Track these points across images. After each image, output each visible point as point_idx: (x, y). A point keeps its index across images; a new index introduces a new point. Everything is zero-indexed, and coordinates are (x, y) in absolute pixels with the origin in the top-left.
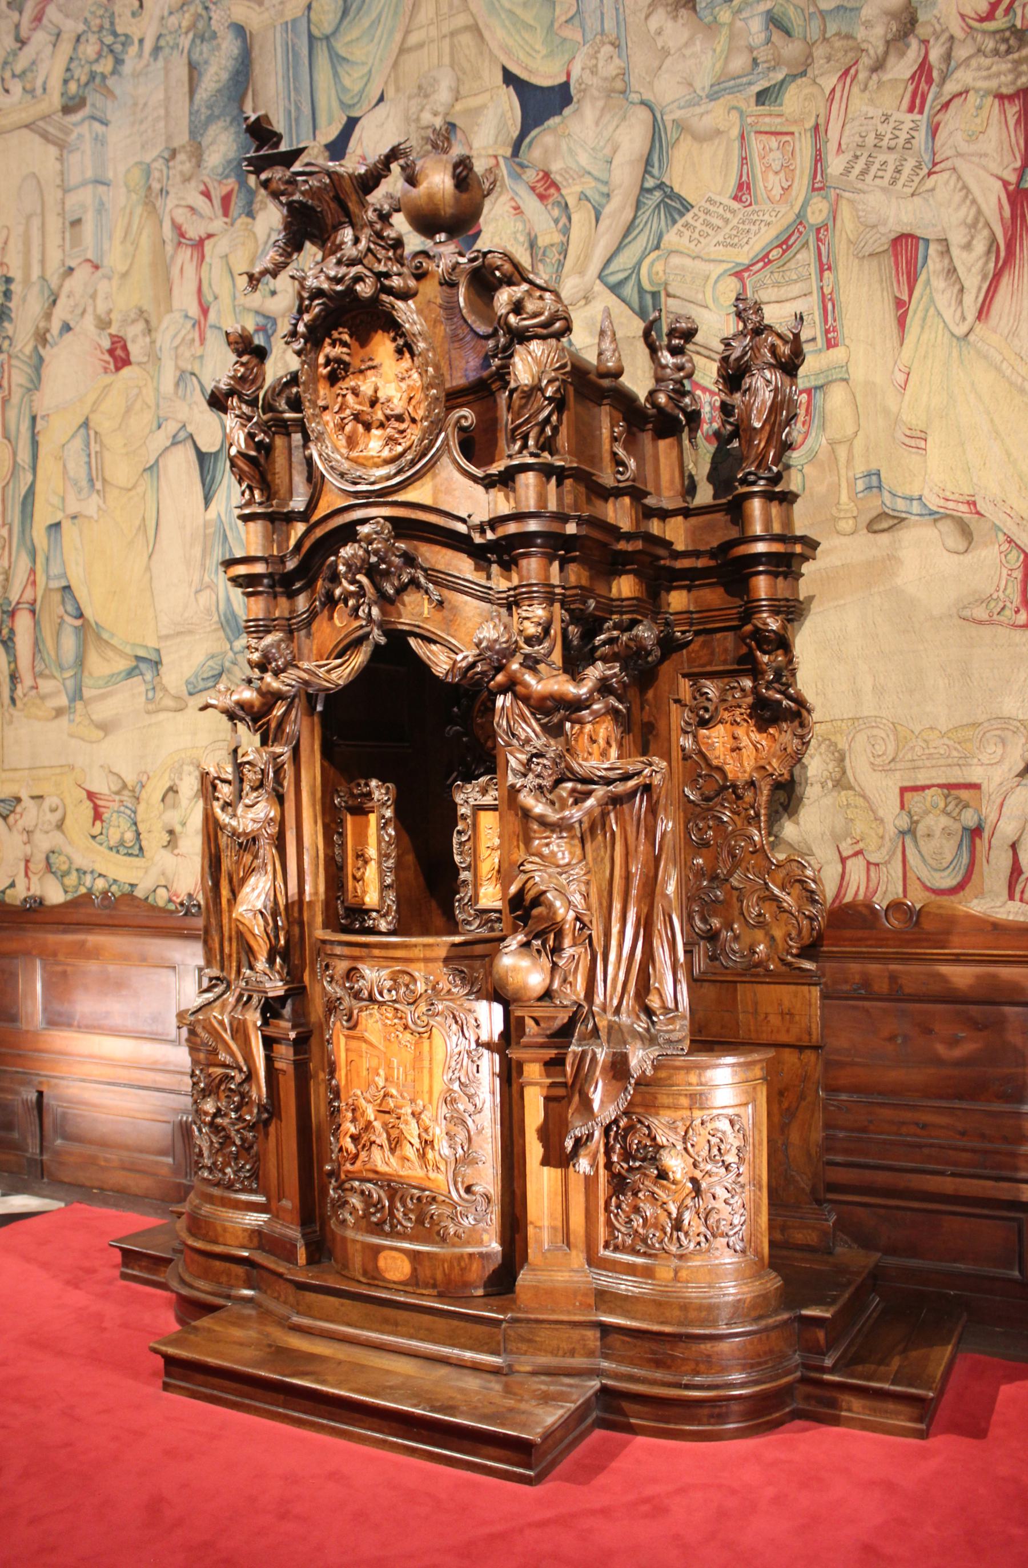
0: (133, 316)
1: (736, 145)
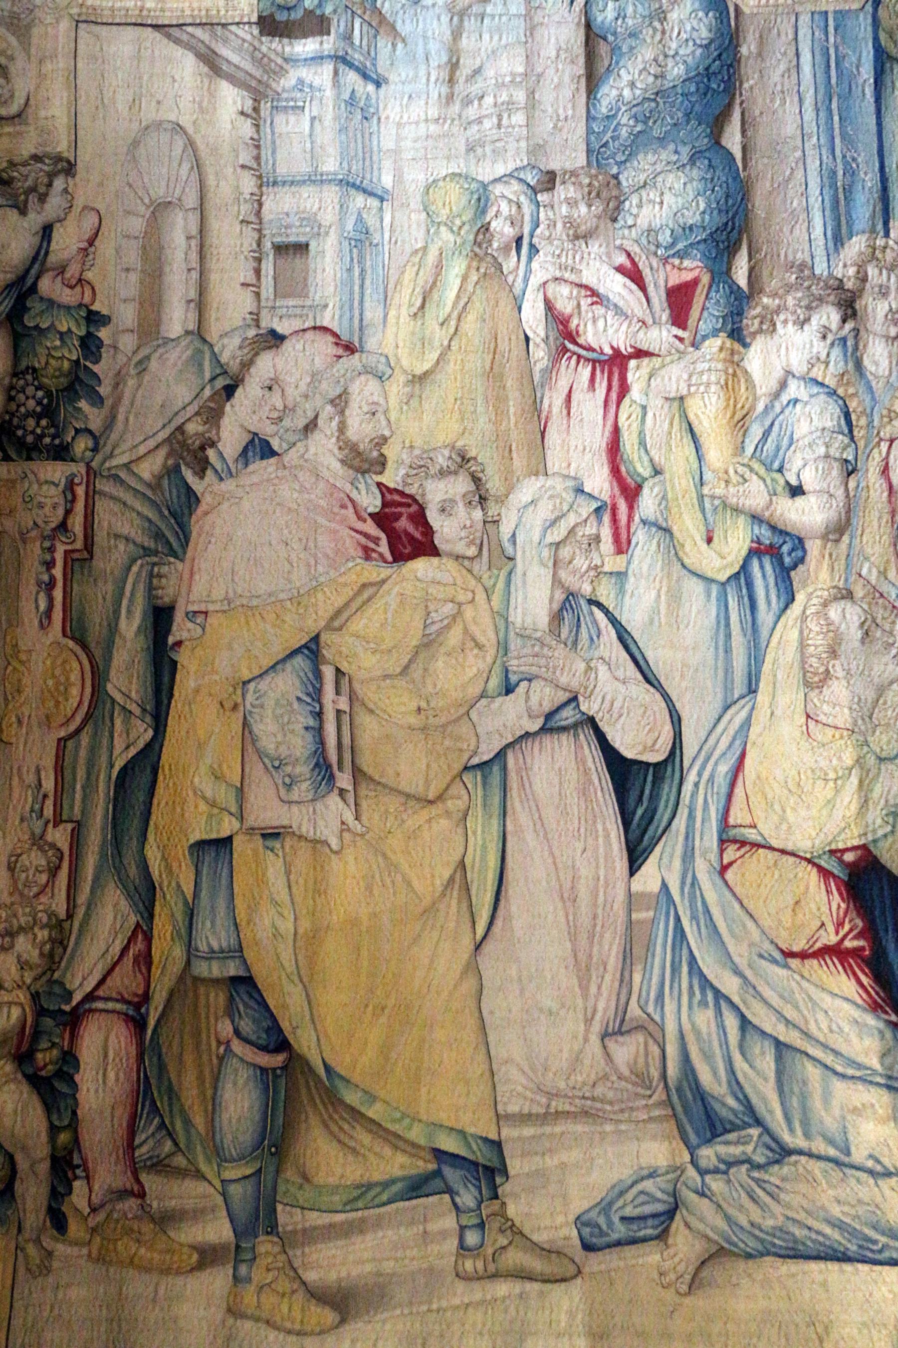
0: (441, 461)
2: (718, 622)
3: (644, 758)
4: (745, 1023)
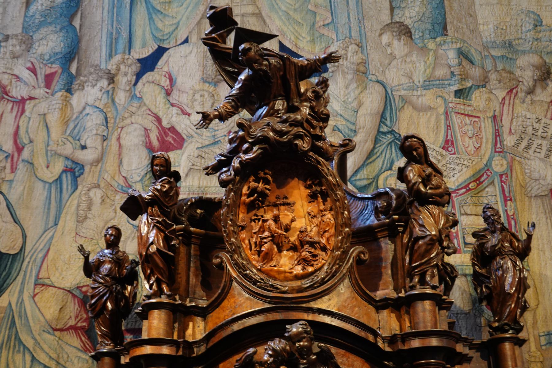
1: (443, 117)
2: (47, 198)
3: (9, 252)
4: (33, 359)
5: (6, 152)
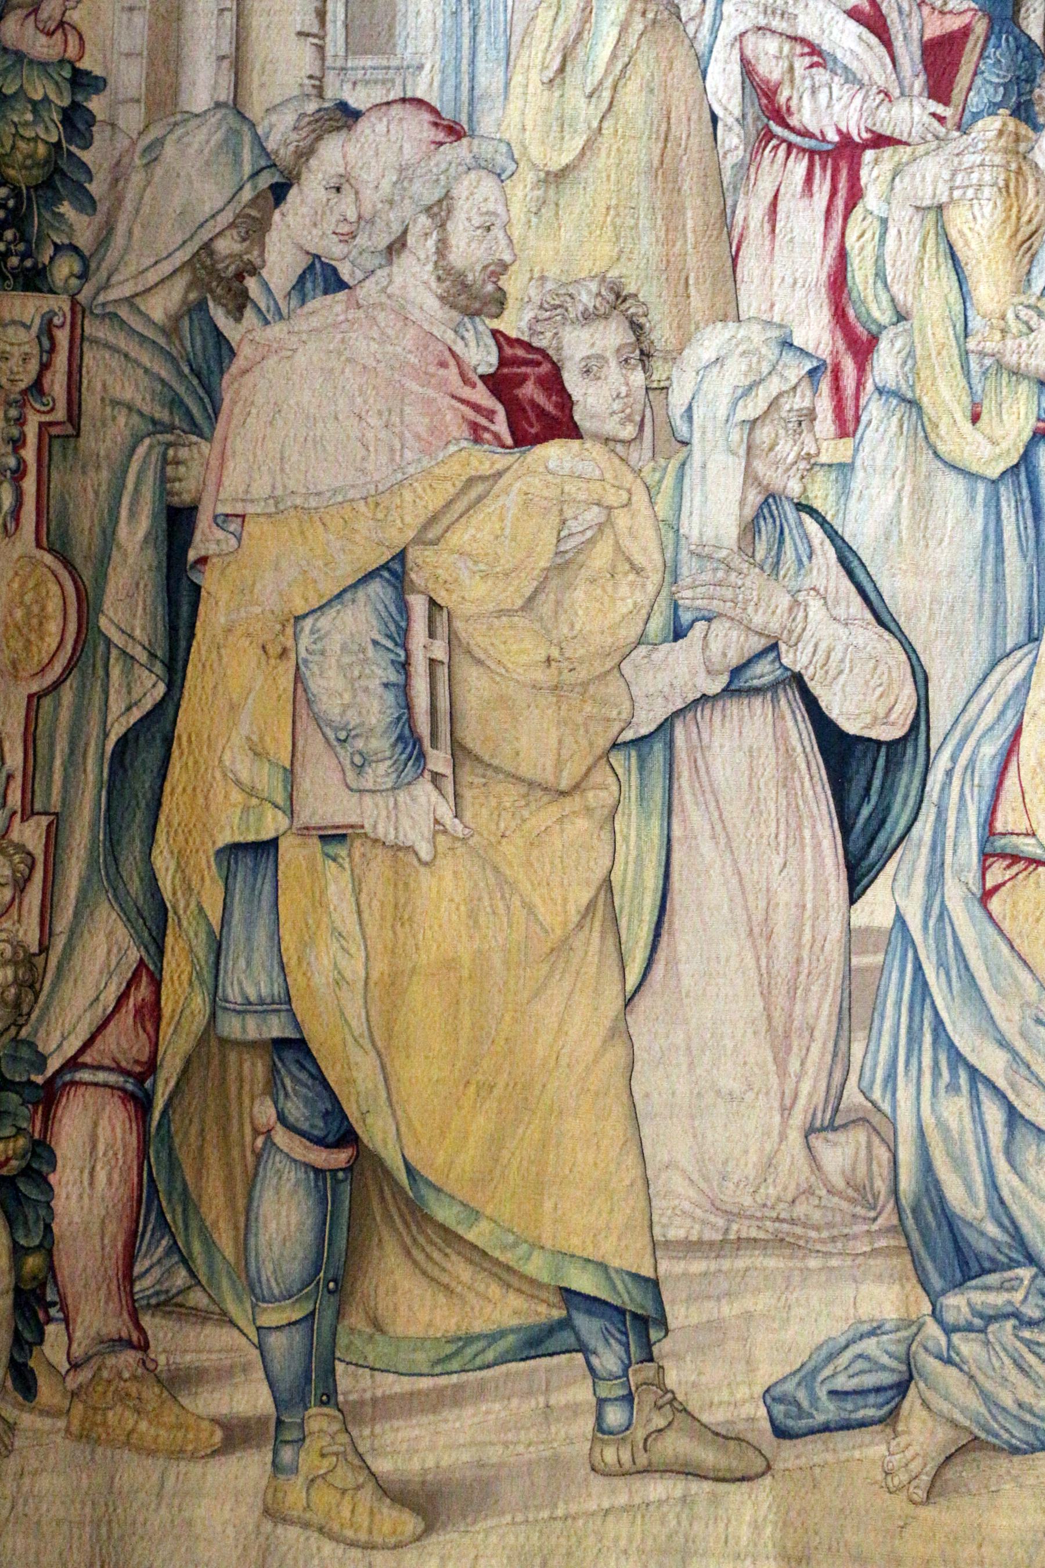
0: (586, 299)
2: (986, 538)
3: (873, 734)
4: (1013, 1117)
5: (808, 355)
